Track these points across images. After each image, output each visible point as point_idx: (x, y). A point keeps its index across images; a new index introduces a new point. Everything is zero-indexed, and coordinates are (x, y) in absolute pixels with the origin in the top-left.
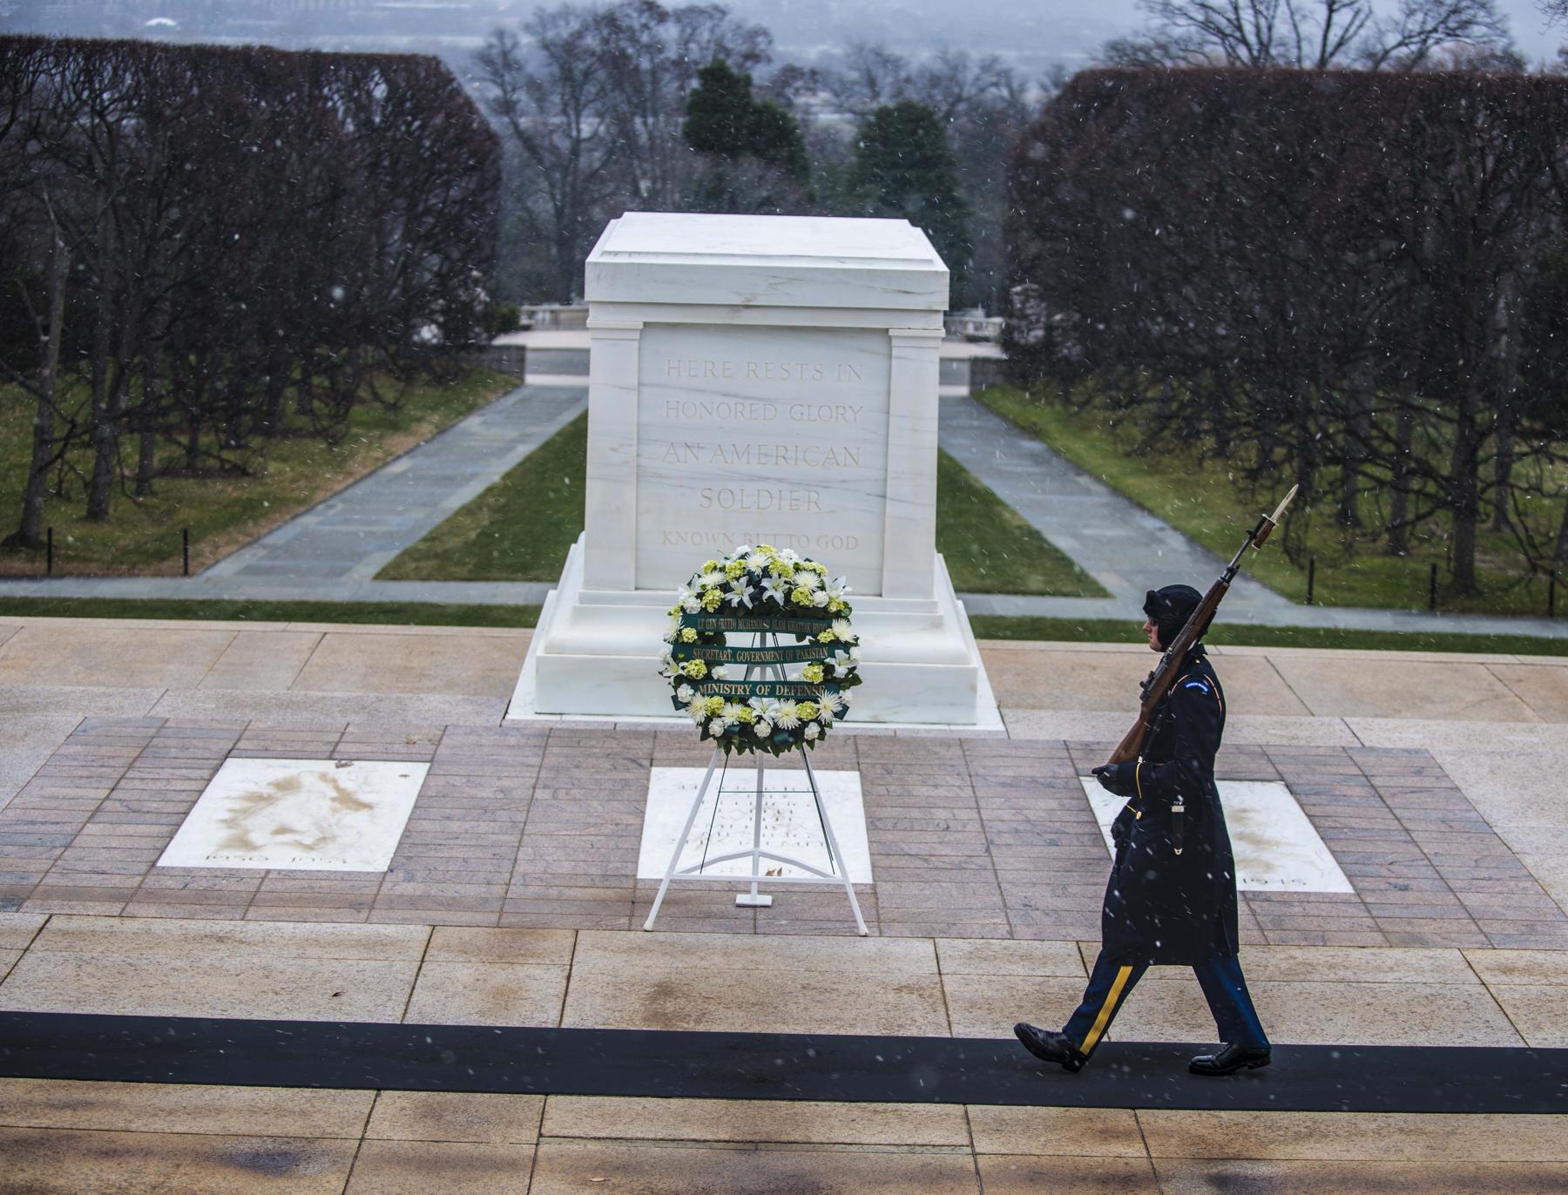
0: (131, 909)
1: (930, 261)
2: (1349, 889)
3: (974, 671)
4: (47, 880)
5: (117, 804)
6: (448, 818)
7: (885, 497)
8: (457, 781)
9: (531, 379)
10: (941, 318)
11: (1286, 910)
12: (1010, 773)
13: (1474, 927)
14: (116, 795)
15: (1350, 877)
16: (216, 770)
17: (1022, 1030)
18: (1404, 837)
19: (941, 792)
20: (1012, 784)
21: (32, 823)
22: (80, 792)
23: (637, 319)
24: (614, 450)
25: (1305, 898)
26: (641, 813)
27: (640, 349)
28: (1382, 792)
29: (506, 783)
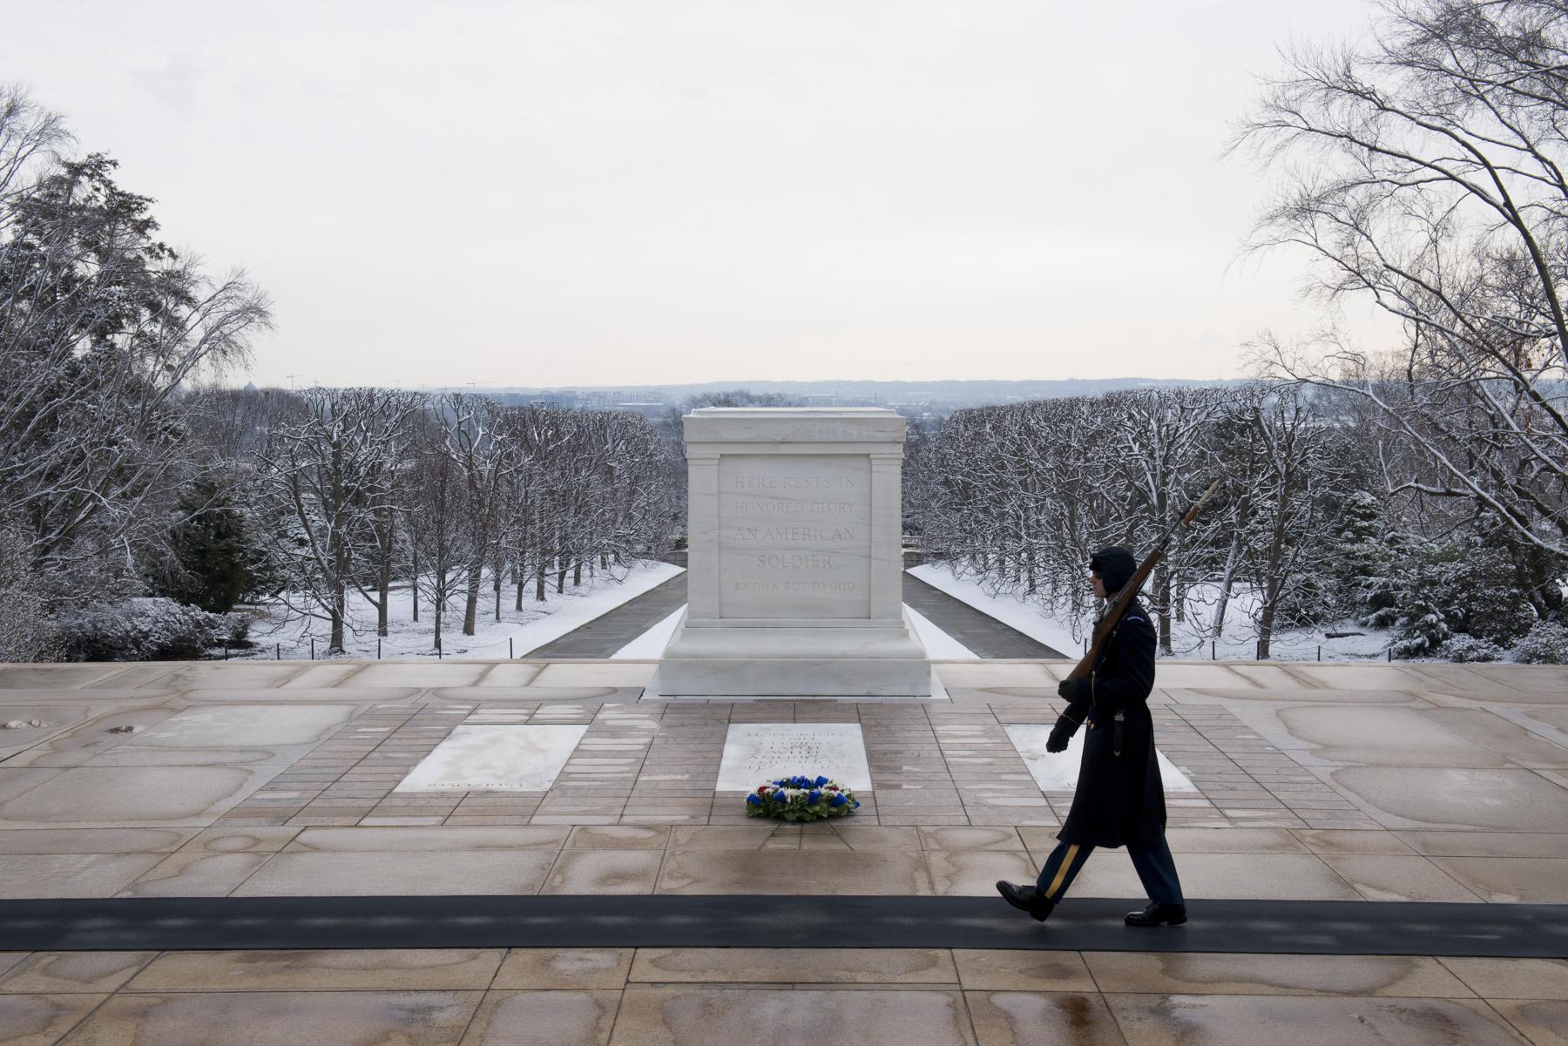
0: (367, 821)
2: (1195, 790)
4: (313, 804)
10: (900, 448)
13: (1292, 815)
14: (380, 748)
15: (1193, 781)
17: (1002, 886)
18: (1222, 756)
19: (913, 734)
21: (316, 767)
22: (355, 748)
23: (717, 451)
24: (704, 533)
26: (722, 751)
27: (719, 471)
28: (1198, 729)
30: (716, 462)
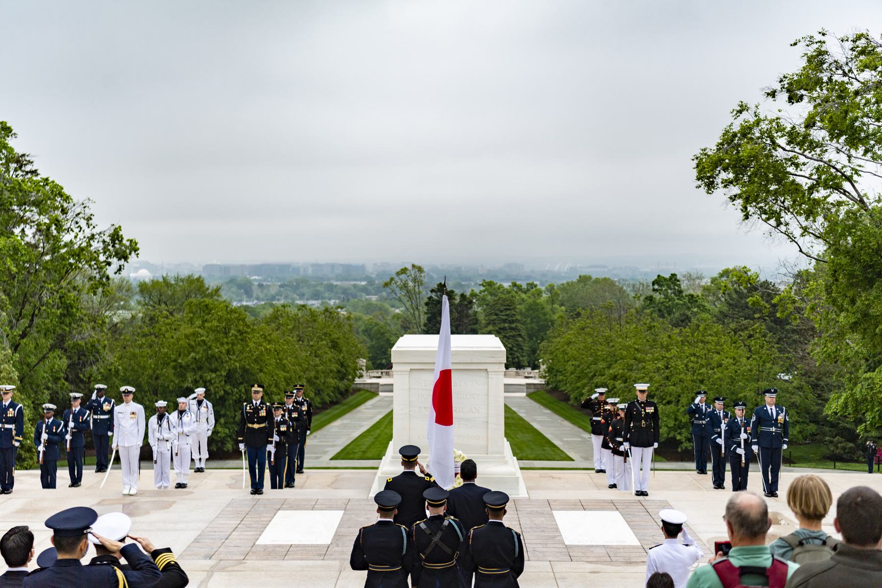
1: (500, 347)
2: (639, 544)
3: (518, 478)
5: (243, 526)
6: (349, 527)
7: (488, 422)
8: (352, 516)
9: (381, 394)
11: (618, 550)
12: (530, 510)
15: (639, 540)
16: (275, 515)
20: (531, 513)
21: (215, 532)
22: (231, 522)
23: (408, 367)
25: (624, 547)
29: (368, 516)
30: (408, 373)
